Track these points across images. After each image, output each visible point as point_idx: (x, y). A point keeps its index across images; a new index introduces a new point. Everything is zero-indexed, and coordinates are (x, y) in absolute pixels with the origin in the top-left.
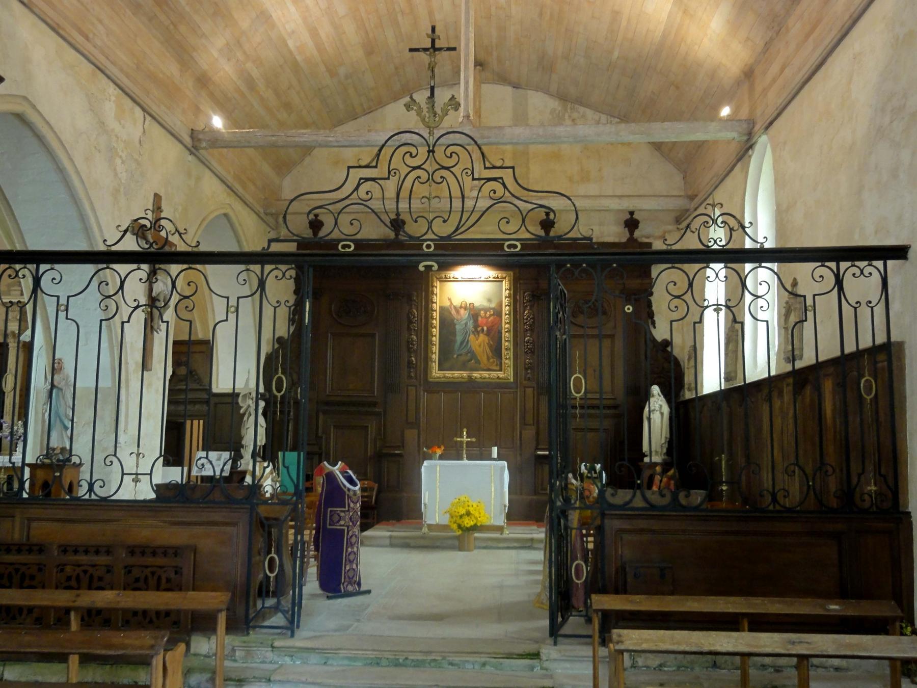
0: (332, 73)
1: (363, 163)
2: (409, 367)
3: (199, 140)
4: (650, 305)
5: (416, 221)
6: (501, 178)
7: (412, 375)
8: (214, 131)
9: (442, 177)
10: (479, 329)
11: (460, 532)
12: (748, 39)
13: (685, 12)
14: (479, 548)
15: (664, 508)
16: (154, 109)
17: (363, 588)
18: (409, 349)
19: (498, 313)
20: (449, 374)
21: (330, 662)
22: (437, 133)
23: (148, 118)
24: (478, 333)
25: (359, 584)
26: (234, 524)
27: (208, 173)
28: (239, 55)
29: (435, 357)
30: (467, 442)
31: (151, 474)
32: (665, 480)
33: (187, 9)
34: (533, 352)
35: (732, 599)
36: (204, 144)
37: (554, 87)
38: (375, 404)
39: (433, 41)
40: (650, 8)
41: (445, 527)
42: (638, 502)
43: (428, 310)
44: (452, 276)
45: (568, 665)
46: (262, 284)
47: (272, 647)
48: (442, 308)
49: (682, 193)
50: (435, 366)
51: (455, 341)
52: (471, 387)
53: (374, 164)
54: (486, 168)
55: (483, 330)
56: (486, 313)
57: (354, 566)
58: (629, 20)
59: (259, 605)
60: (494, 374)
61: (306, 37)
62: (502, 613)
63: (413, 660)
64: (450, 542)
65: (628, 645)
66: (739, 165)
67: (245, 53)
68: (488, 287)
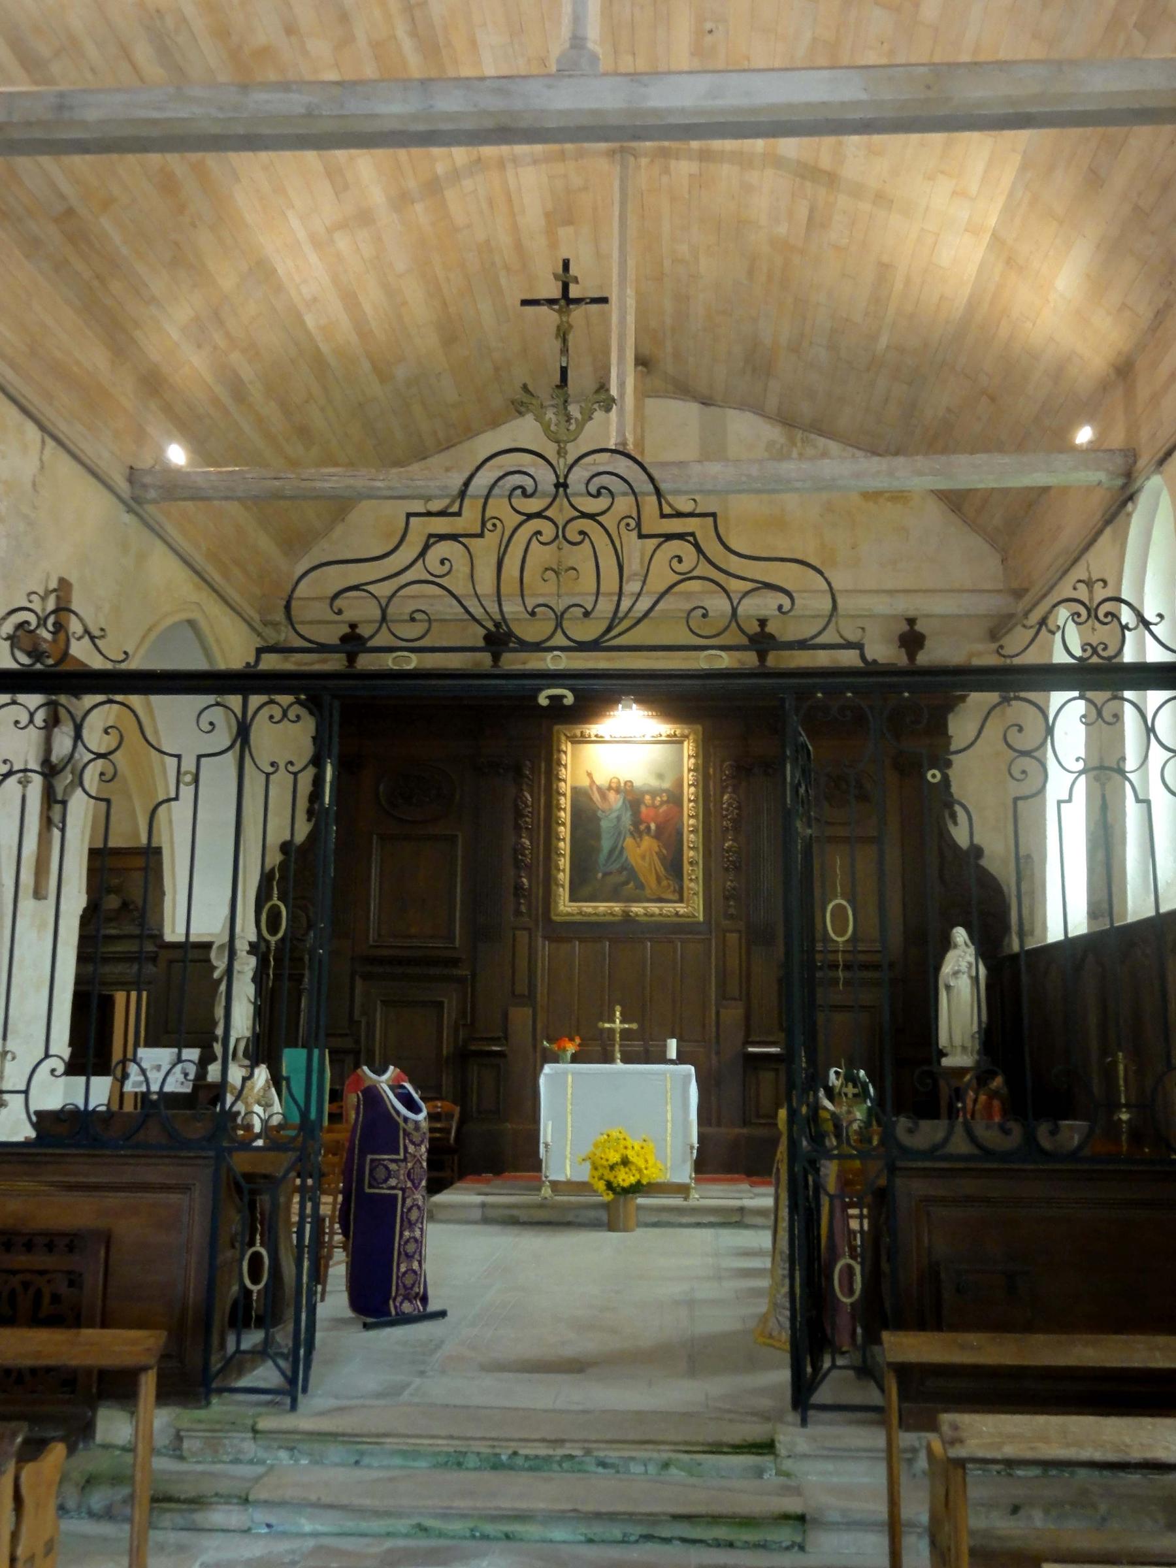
0: (384, 376)
3: (144, 486)
6: (692, 534)
7: (523, 909)
8: (169, 471)
9: (582, 533)
10: (642, 827)
11: (609, 1197)
12: (1124, 306)
13: (1009, 261)
14: (647, 1225)
15: (1005, 1156)
16: (63, 428)
17: (433, 1307)
20: (588, 907)
21: (366, 1460)
22: (573, 452)
23: (50, 443)
24: (640, 834)
25: (424, 1299)
26: (185, 1189)
27: (160, 547)
28: (219, 339)
30: (623, 1031)
31: (26, 1092)
33: (125, 251)
34: (737, 869)
35: (1161, 1340)
36: (152, 494)
37: (772, 403)
38: (455, 962)
39: (565, 288)
40: (945, 257)
41: (582, 1187)
42: (960, 1145)
45: (830, 1467)
46: (243, 732)
47: (255, 1431)
48: (575, 790)
49: (1001, 586)
50: (563, 893)
51: (598, 850)
52: (625, 932)
53: (455, 508)
54: (663, 516)
55: (648, 828)
57: (415, 1266)
58: (908, 282)
59: (231, 1347)
60: (669, 908)
61: (335, 308)
62: (696, 1356)
63: (527, 1457)
64: (592, 1214)
65: (972, 1447)
66: (1108, 531)
67: (228, 335)
68: (657, 754)
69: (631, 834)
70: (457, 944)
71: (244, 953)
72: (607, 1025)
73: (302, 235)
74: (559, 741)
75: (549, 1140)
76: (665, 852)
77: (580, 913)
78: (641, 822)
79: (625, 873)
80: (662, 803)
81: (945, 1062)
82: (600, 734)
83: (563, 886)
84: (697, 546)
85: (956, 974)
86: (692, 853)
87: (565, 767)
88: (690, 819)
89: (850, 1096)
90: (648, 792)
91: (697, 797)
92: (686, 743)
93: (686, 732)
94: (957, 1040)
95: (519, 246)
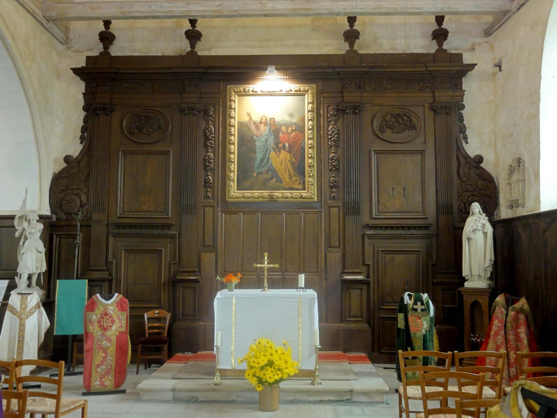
2: (205, 186)
4: (461, 119)
7: (209, 194)
10: (280, 145)
11: (260, 389)
14: (286, 402)
18: (205, 166)
19: (301, 129)
20: (248, 193)
24: (279, 150)
29: (234, 175)
30: (270, 270)
32: (512, 313)
34: (338, 170)
38: (169, 226)
43: (225, 126)
44: (251, 89)
48: (240, 123)
51: (254, 159)
52: (270, 208)
55: (284, 146)
56: (287, 129)
60: (296, 193)
68: (290, 102)
69: (274, 149)
70: (170, 216)
71: (35, 221)
72: (259, 265)
74: (230, 94)
75: (219, 344)
76: (294, 160)
77: (244, 197)
78: (280, 143)
79: (270, 173)
80: (292, 131)
81: (467, 285)
82: (255, 90)
83: (233, 180)
85: (474, 231)
86: (310, 161)
87: (234, 109)
88: (309, 141)
89: (419, 310)
90: (284, 125)
91: (313, 127)
92: (306, 95)
93: (307, 88)
94: (475, 272)
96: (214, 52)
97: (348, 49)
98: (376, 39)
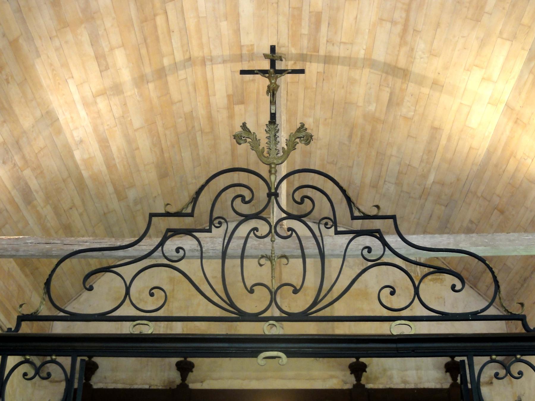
0: (121, 196)
1: (172, 209)
5: (251, 291)
6: (378, 231)
9: (289, 229)
28: (17, 158)
40: (474, 122)
53: (189, 210)
54: (354, 218)
58: (449, 138)
67: (24, 157)
73: (77, 97)
84: (382, 239)
95: (210, 118)
96: (208, 385)
97: (355, 382)
98: (385, 370)
